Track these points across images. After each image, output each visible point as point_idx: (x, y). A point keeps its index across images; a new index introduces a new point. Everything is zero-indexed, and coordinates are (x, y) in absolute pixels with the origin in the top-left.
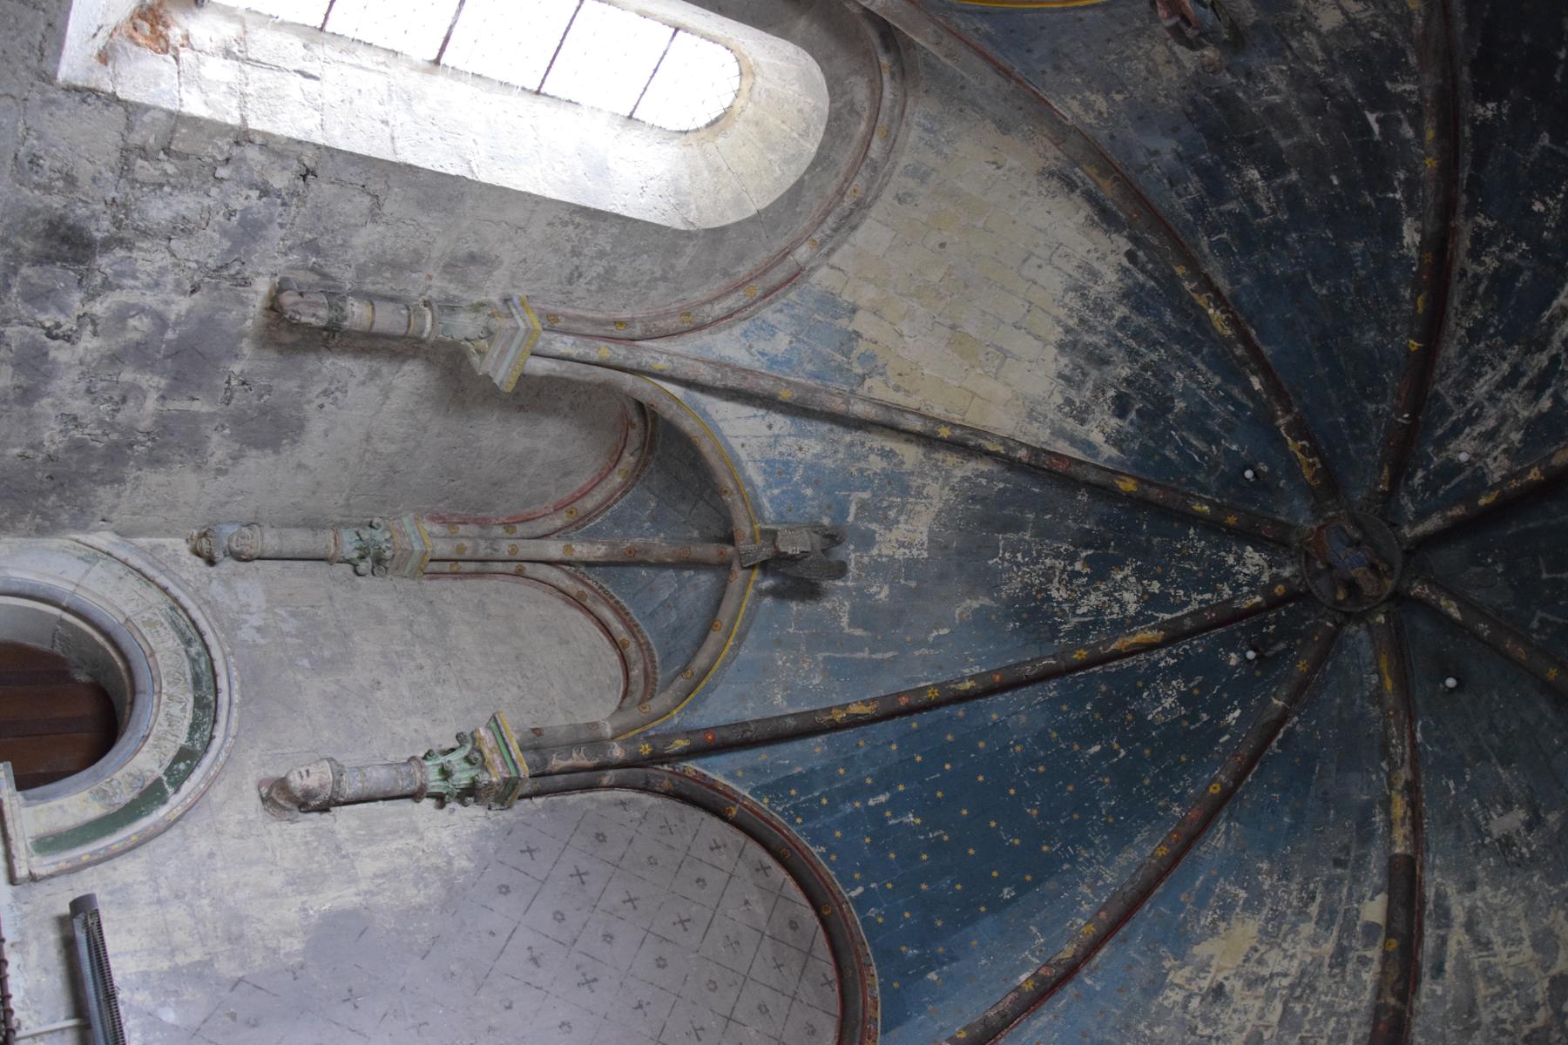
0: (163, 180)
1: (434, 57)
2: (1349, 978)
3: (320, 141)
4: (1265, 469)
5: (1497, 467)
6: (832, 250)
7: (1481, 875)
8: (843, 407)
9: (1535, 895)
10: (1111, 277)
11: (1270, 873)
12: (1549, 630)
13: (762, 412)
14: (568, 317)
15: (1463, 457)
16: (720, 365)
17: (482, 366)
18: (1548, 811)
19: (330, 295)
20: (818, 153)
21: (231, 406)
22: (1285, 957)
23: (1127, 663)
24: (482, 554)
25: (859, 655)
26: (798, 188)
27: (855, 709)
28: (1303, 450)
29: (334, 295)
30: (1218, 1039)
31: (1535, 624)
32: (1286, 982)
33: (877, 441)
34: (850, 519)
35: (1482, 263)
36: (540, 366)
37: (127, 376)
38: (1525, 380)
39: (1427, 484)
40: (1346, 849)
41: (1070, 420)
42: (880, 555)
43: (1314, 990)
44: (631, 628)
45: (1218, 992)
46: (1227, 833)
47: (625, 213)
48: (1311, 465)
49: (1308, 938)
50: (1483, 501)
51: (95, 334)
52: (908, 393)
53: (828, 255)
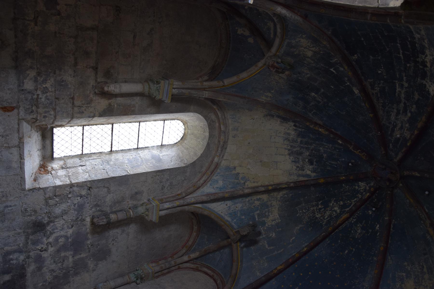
0: (57, 203)
1: (110, 150)
3: (90, 180)
4: (354, 161)
6: (223, 156)
8: (243, 192)
10: (293, 133)
13: (223, 202)
14: (165, 198)
15: (398, 136)
16: (208, 195)
17: (149, 218)
19: (105, 216)
20: (209, 135)
21: (91, 252)
23: (344, 225)
24: (167, 267)
25: (274, 254)
26: (208, 145)
27: (279, 268)
28: (360, 152)
29: (106, 215)
33: (255, 197)
34: (257, 219)
35: (376, 90)
36: (163, 213)
37: (63, 254)
38: (401, 111)
41: (300, 171)
42: (268, 226)
44: (213, 271)
47: (169, 168)
50: (408, 144)
51: (52, 247)
52: (257, 182)
53: (223, 157)
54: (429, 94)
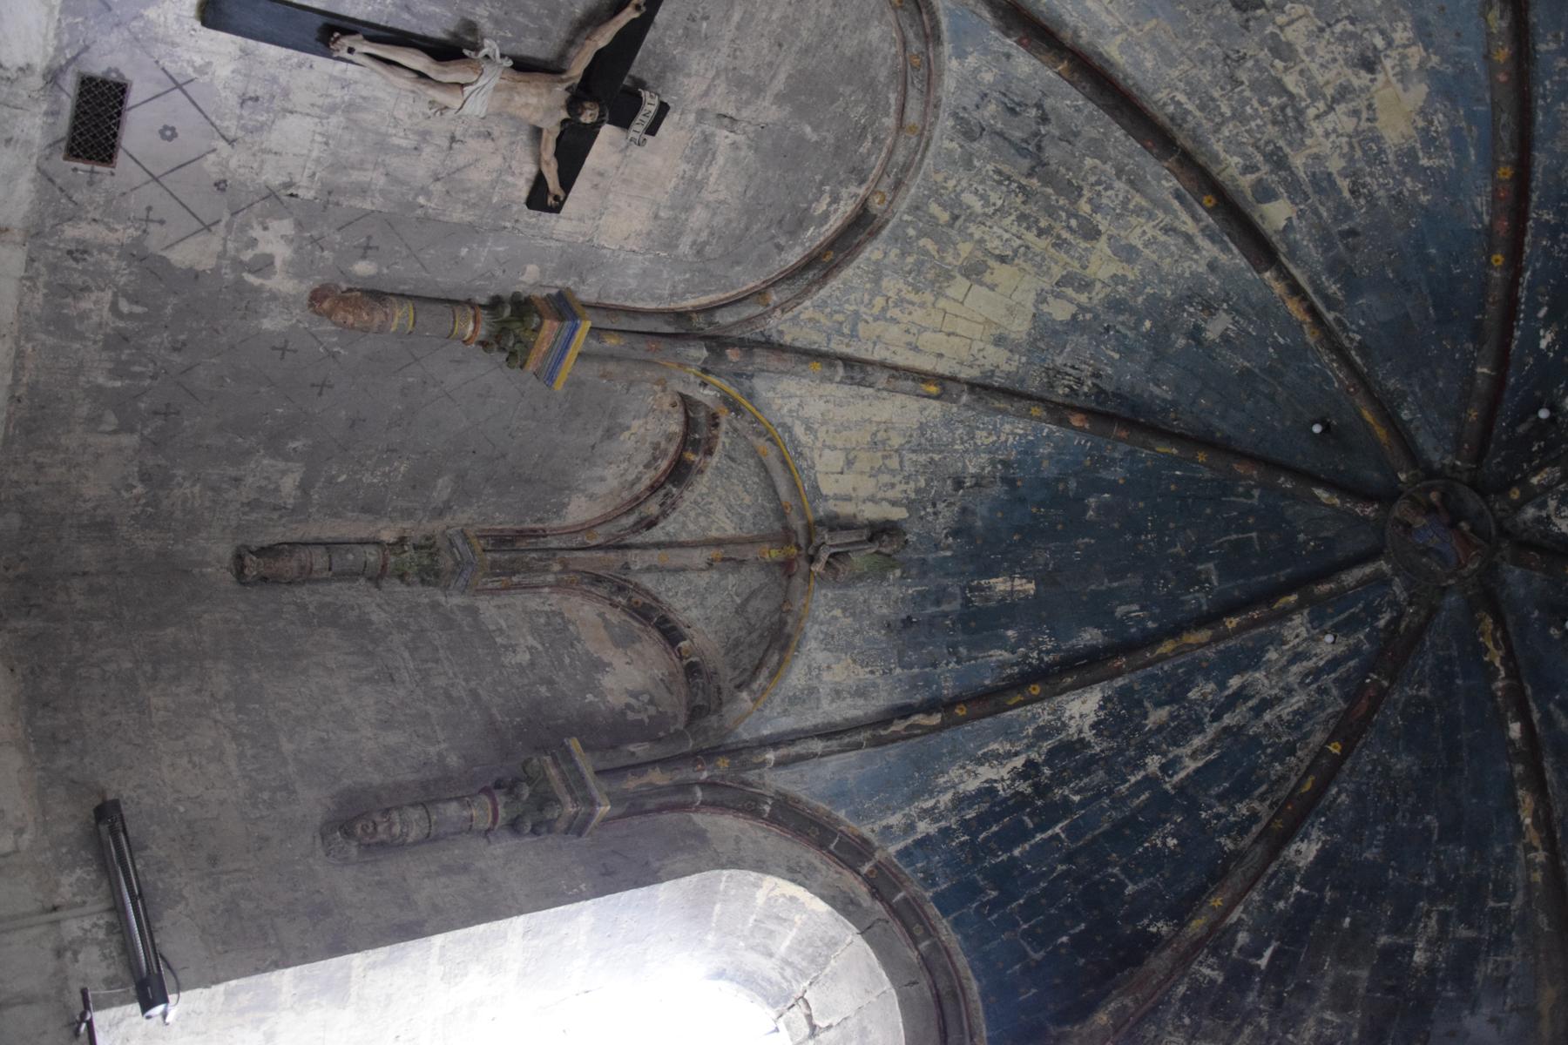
2: (1250, 149)
4: (1553, 631)
5: (1297, 628)
7: (1211, 278)
9: (1161, 281)
11: (1414, 194)
12: (1241, 489)
18: (1188, 345)
22: (1335, 130)
30: (1322, 30)
31: (1256, 493)
32: (1311, 112)
38: (1250, 704)
39: (1375, 614)
40: (1352, 249)
43: (1275, 123)
45: (1369, 64)
46: (1479, 215)
48: (1482, 634)
49: (1326, 157)
50: (1293, 598)
54: (1106, 700)
